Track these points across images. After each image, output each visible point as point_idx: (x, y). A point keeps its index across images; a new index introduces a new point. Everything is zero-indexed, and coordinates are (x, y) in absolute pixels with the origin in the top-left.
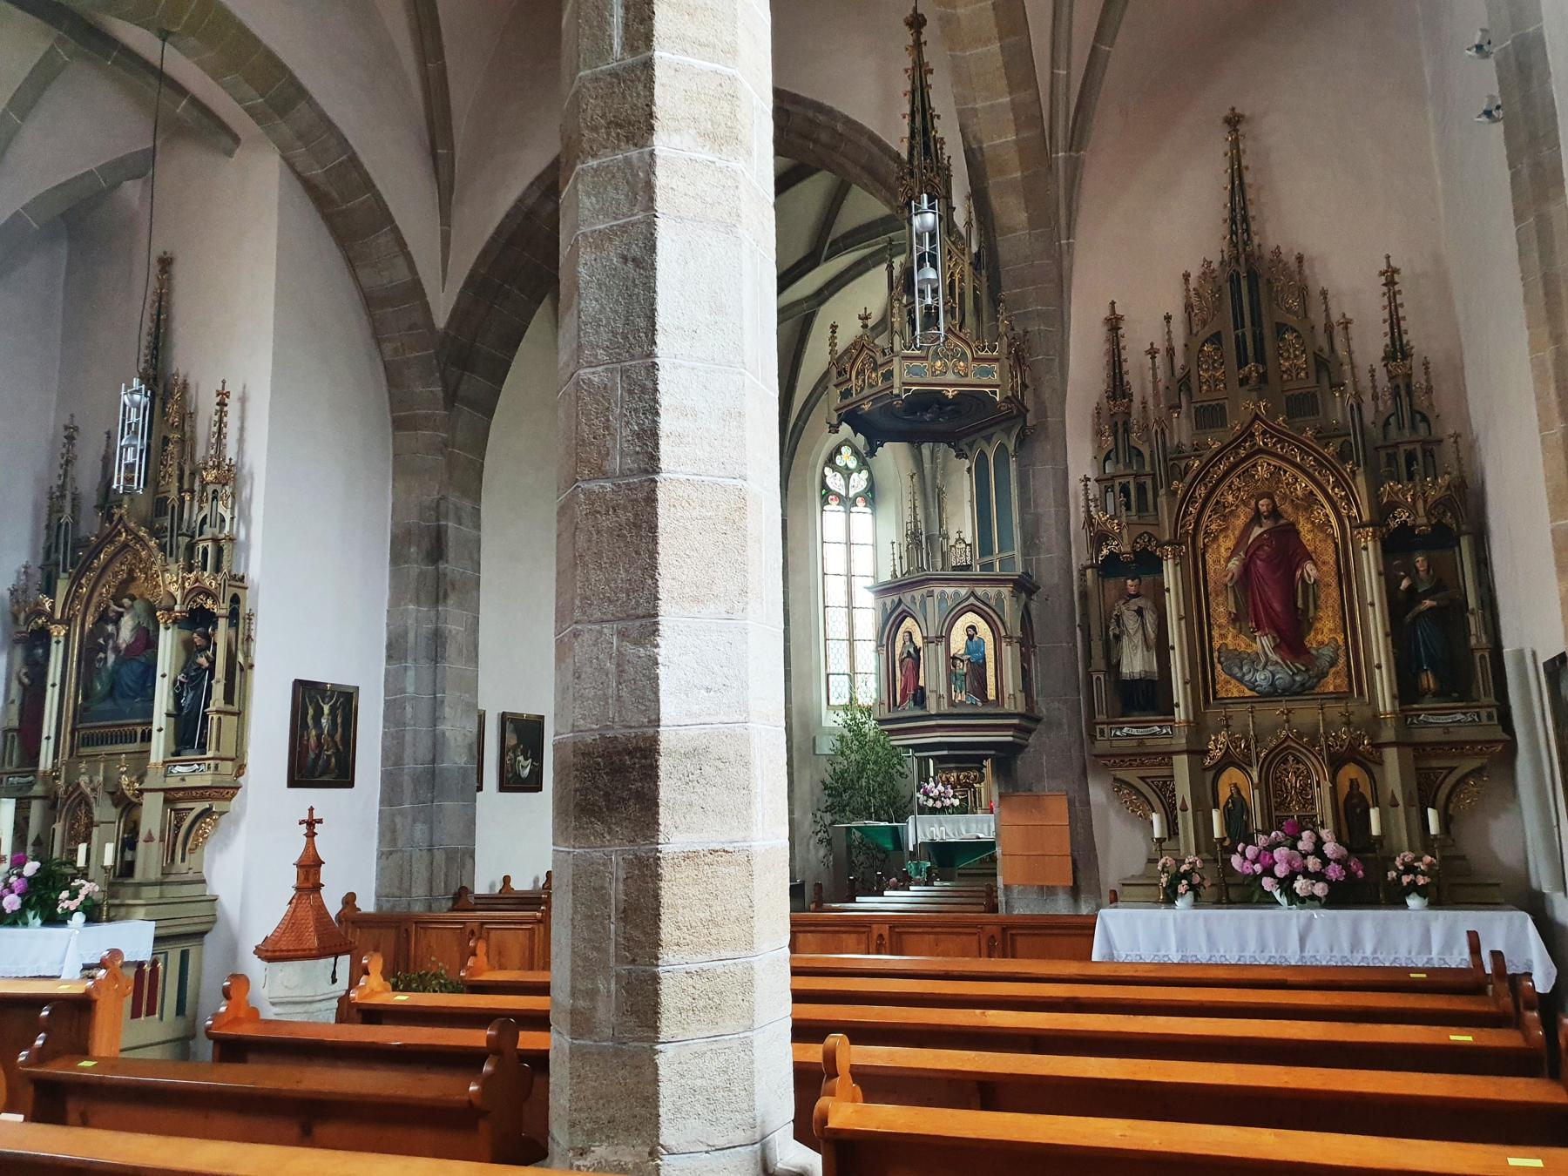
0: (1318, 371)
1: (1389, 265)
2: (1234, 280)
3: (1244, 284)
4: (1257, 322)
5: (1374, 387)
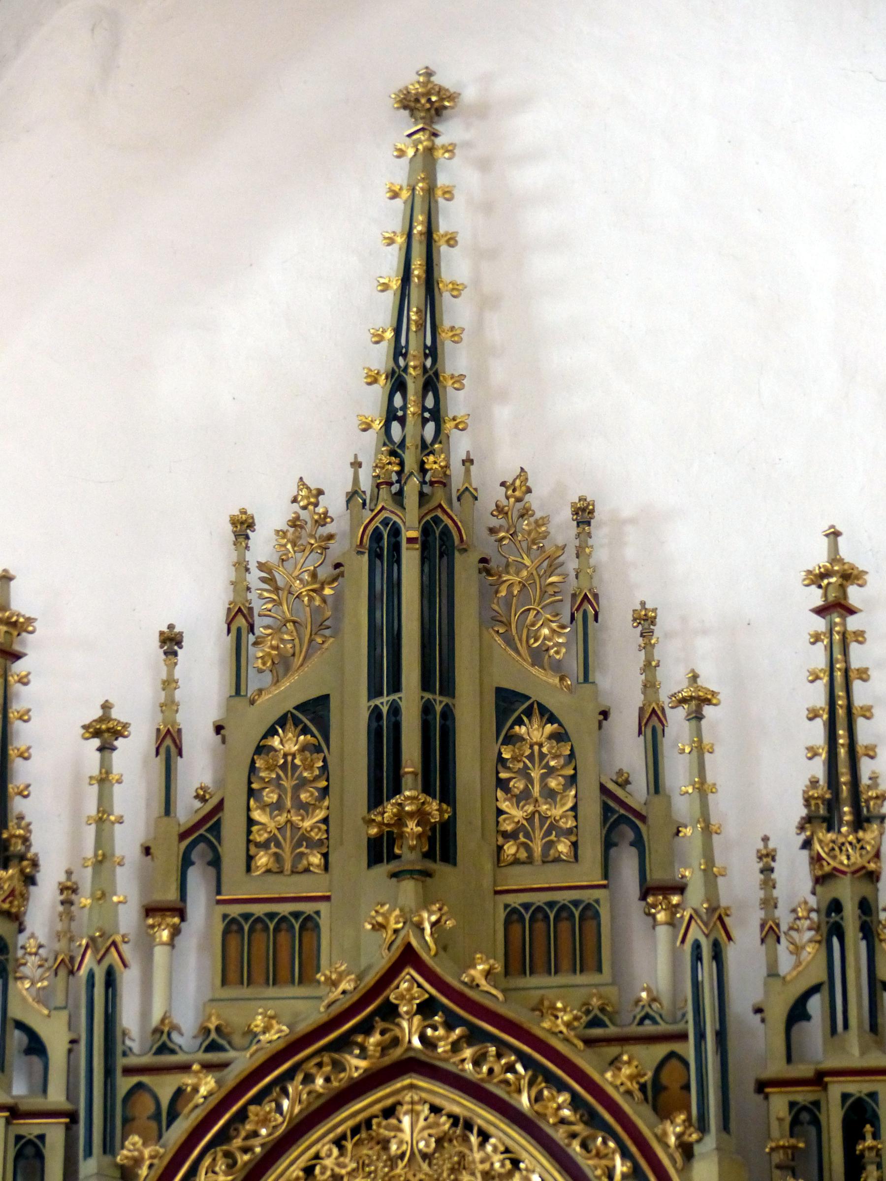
0: (608, 844)
1: (835, 558)
3: (410, 559)
5: (769, 903)
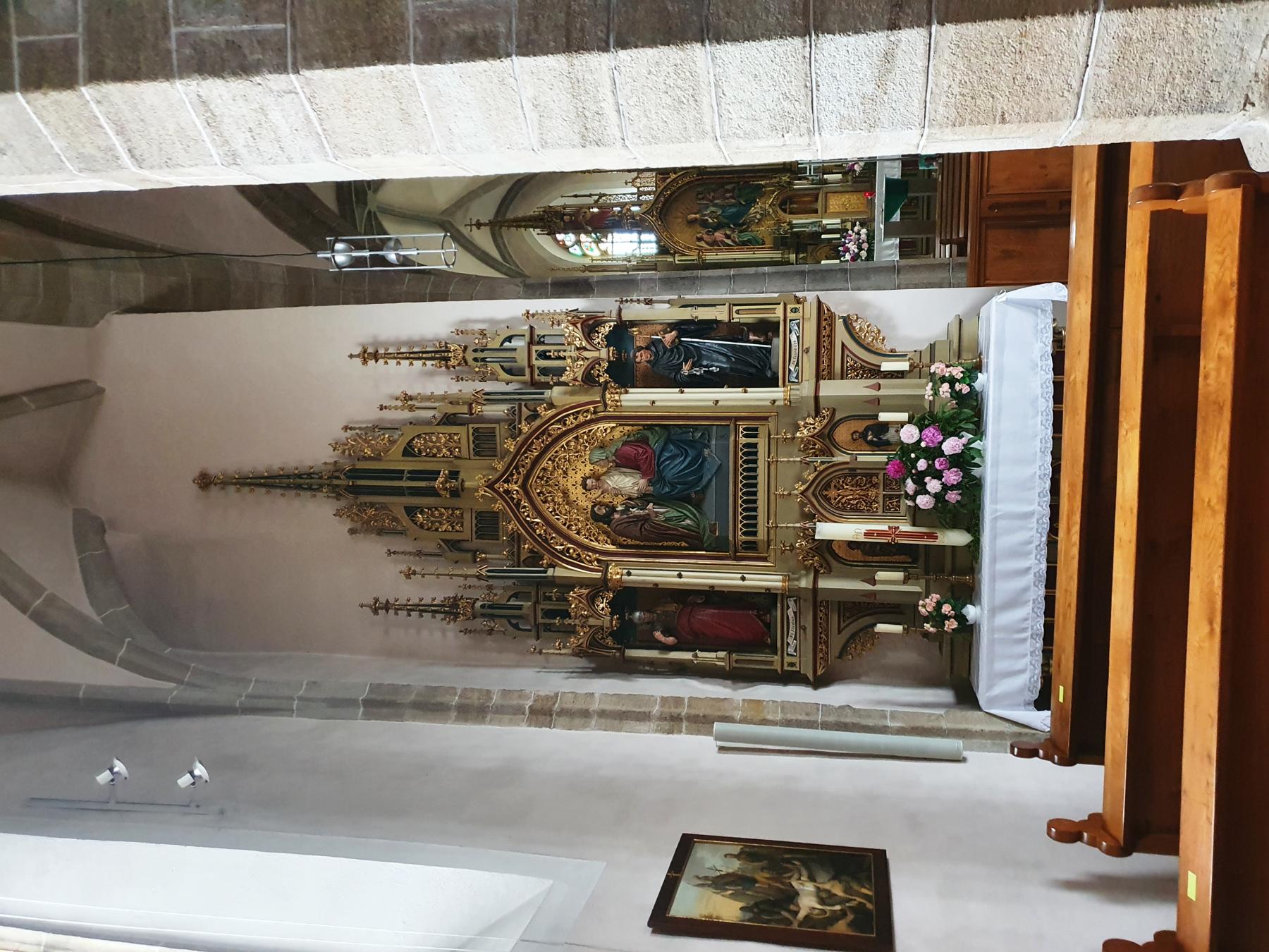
2: (356, 491)
4: (398, 474)
